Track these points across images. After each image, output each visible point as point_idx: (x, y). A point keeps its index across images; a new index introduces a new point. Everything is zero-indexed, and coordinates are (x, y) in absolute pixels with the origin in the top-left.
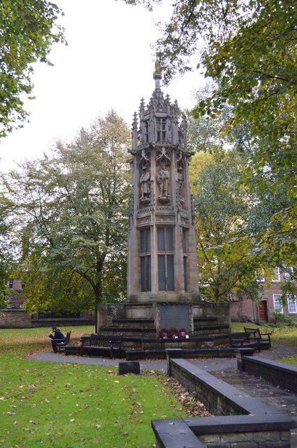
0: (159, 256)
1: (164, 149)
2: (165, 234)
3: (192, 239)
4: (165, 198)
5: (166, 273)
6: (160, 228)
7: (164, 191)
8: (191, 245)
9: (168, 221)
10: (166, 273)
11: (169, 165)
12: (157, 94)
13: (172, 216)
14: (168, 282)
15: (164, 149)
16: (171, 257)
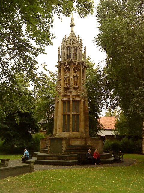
0: (64, 116)
1: (67, 63)
2: (66, 104)
3: (82, 106)
4: (66, 87)
5: (66, 124)
6: (64, 102)
7: (66, 84)
8: (82, 109)
9: (67, 98)
10: (66, 124)
11: (69, 70)
12: (72, 33)
13: (69, 96)
14: (65, 128)
15: (67, 63)
16: (69, 115)
